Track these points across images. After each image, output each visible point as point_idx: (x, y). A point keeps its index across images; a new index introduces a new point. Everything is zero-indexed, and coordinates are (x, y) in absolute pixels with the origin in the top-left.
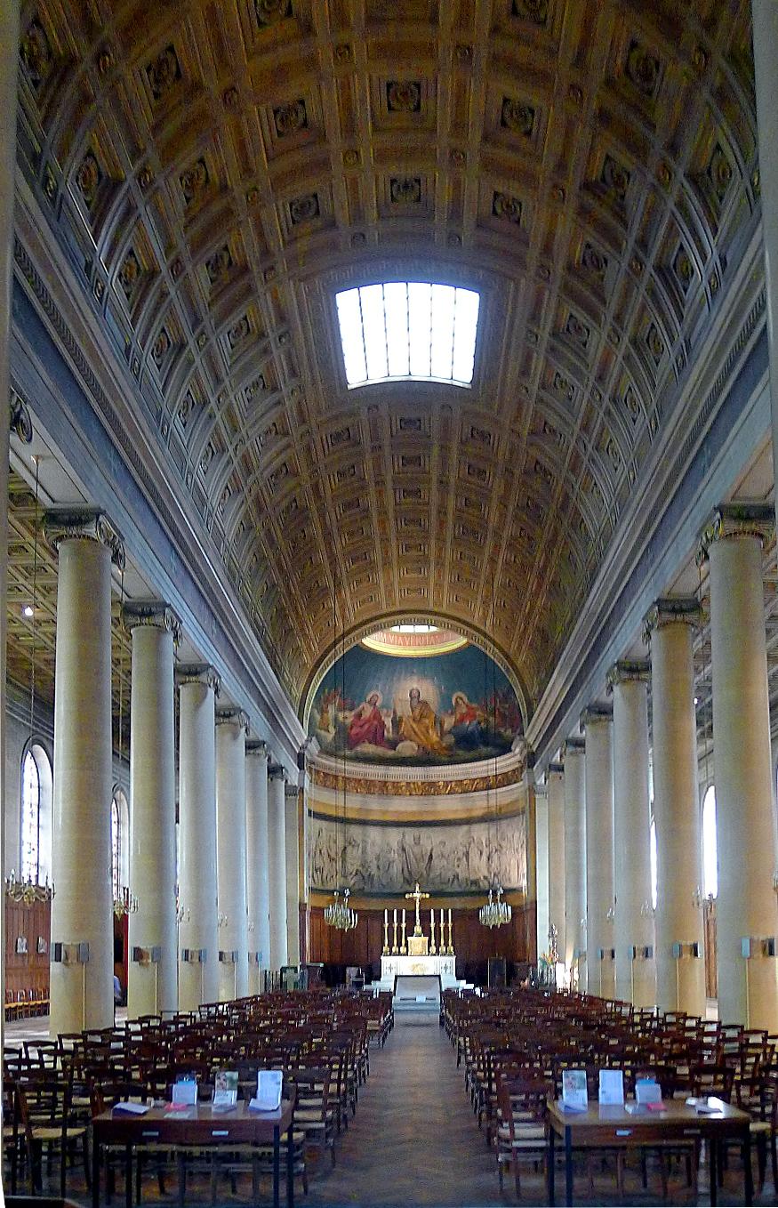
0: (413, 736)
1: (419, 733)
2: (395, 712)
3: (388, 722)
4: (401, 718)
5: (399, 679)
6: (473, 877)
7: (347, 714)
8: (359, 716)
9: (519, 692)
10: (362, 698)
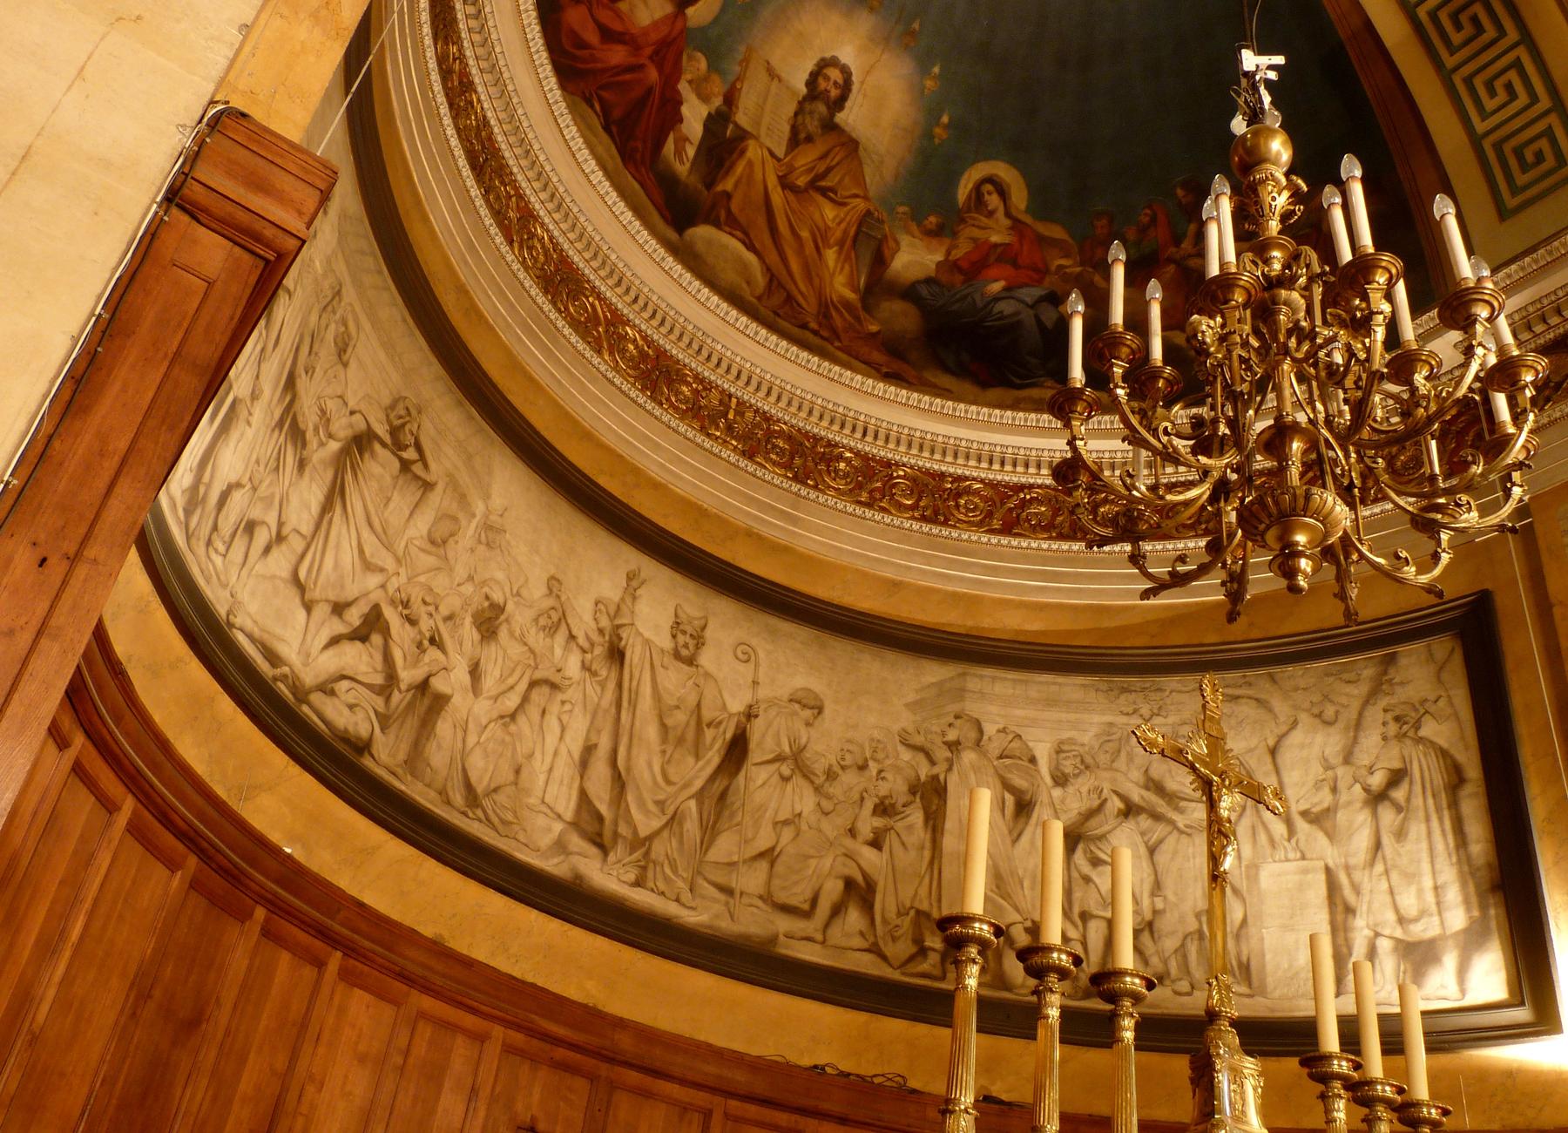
2: (730, 99)
3: (694, 115)
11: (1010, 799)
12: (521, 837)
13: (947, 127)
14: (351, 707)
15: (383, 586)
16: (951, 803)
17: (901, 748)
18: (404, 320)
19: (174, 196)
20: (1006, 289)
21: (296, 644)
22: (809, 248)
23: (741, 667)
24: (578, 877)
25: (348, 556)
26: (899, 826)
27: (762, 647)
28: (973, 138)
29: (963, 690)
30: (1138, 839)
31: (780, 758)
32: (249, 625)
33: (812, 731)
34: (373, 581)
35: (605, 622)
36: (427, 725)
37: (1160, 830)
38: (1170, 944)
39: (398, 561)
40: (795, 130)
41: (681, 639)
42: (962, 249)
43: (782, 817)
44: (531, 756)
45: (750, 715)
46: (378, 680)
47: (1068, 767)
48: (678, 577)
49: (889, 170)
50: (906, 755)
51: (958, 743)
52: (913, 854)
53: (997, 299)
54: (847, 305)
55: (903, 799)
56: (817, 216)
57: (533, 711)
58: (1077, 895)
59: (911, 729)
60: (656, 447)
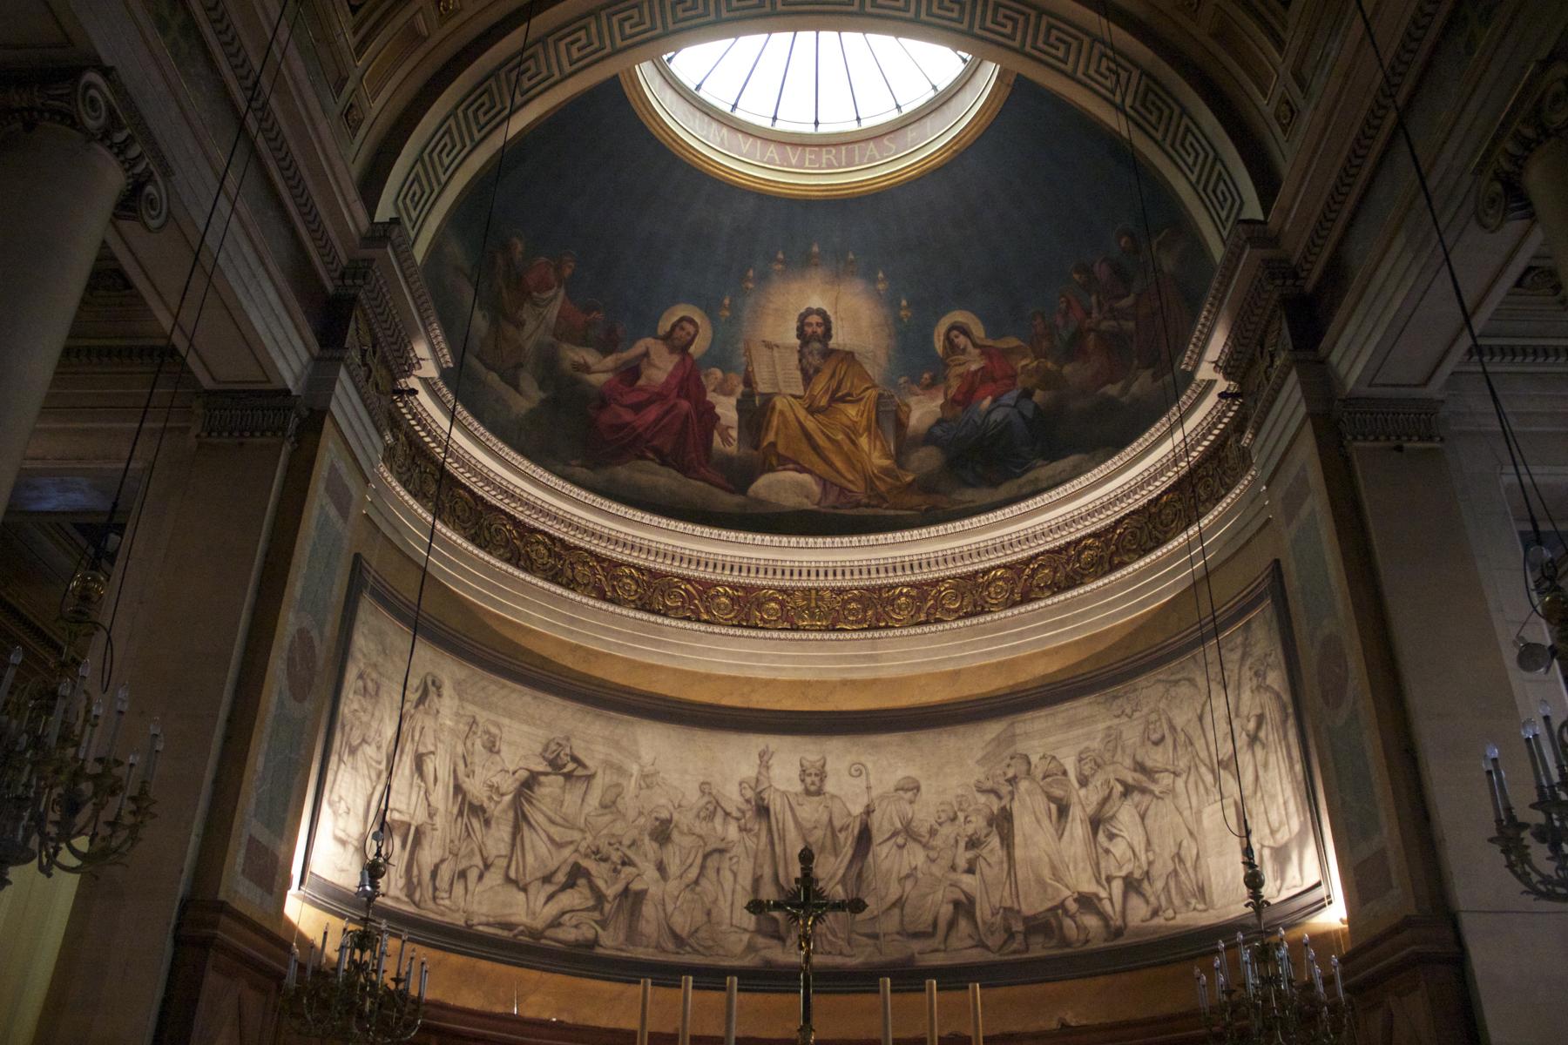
0: (812, 459)
1: (821, 441)
2: (748, 381)
3: (727, 410)
4: (768, 398)
5: (764, 278)
6: (1033, 904)
10: (646, 326)
11: (1053, 807)
12: (721, 952)
13: (909, 305)
14: (576, 926)
15: (576, 851)
16: (1016, 823)
17: (978, 795)
18: (535, 698)
19: (178, 941)
20: (994, 401)
21: (523, 912)
22: (847, 446)
23: (856, 781)
24: (768, 963)
25: (543, 848)
26: (985, 852)
27: (869, 761)
28: (929, 306)
29: (1014, 735)
30: (1134, 812)
31: (895, 834)
32: (484, 919)
33: (916, 806)
34: (567, 852)
35: (749, 794)
37: (1147, 799)
38: (1159, 885)
39: (582, 830)
40: (804, 371)
41: (808, 780)
42: (955, 384)
43: (904, 872)
44: (715, 902)
45: (869, 811)
46: (591, 903)
47: (1087, 770)
48: (798, 739)
49: (883, 360)
50: (982, 799)
51: (1015, 777)
52: (996, 869)
53: (989, 412)
54: (886, 471)
55: (984, 832)
56: (845, 420)
57: (711, 873)
58: (1103, 864)
59: (982, 778)
60: (760, 657)
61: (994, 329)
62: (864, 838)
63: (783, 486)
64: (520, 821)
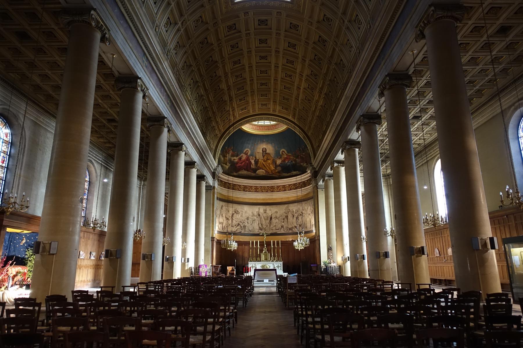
2: (255, 158)
4: (258, 160)
5: (257, 144)
7: (235, 158)
8: (240, 159)
9: (309, 147)
36: (245, 228)
61: (288, 152)
62: (271, 218)
63: (261, 172)
64: (232, 219)
